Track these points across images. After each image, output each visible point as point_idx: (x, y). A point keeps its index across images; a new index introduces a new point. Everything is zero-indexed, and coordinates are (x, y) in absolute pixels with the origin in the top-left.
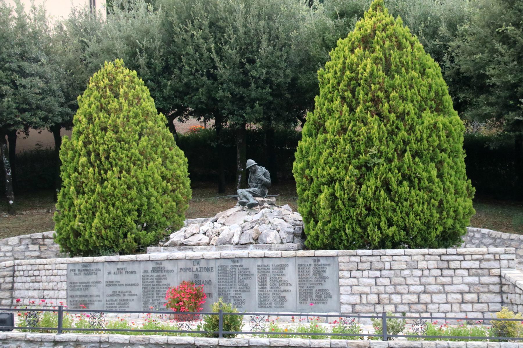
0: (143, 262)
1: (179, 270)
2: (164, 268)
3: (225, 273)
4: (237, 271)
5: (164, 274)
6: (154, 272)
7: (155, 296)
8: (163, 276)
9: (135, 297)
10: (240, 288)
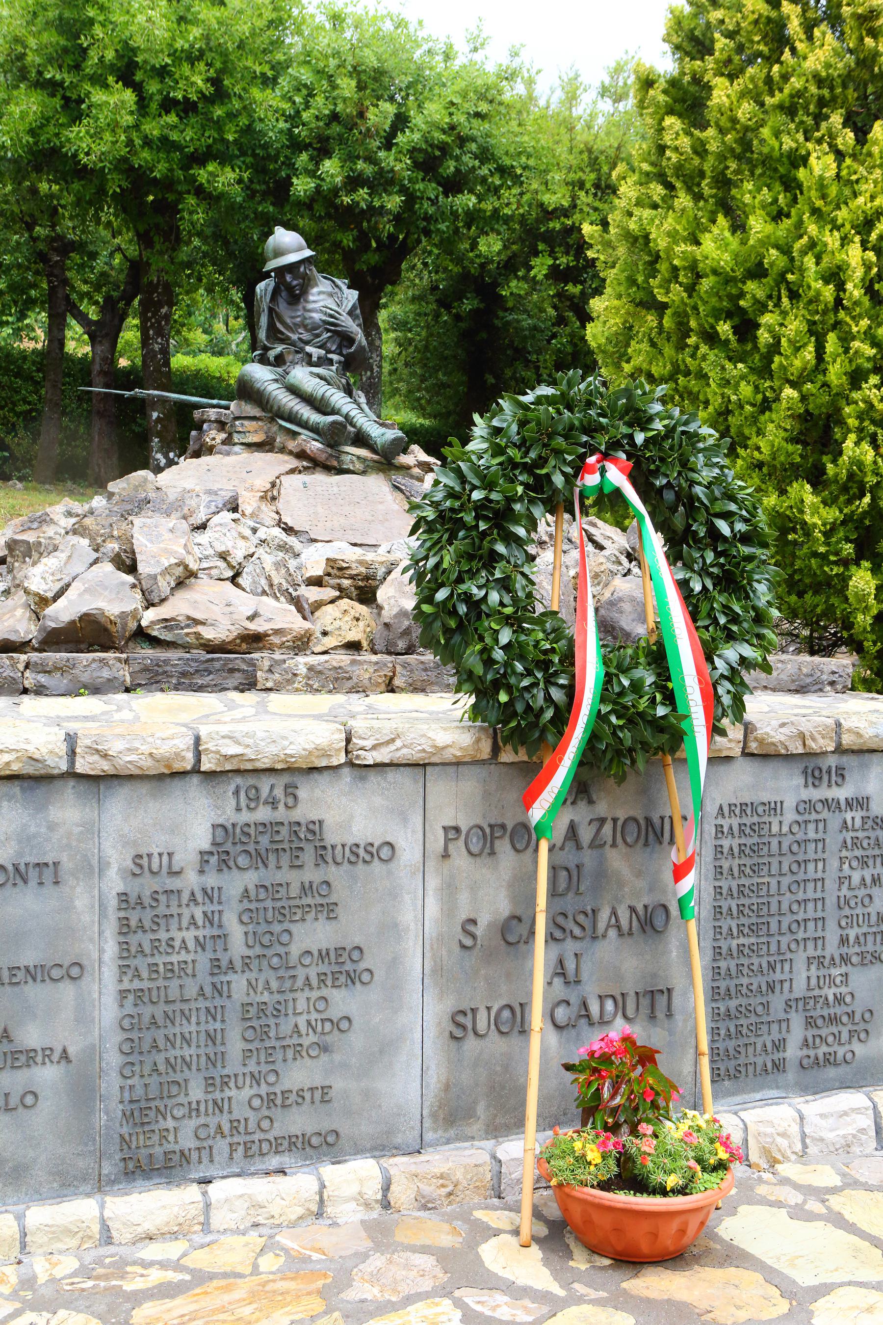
0: (124, 792)
1: (437, 840)
2: (315, 829)
3: (755, 849)
4: (833, 840)
5: (311, 874)
6: (224, 864)
7: (235, 1046)
8: (306, 889)
9: (47, 1076)
10: (844, 941)
